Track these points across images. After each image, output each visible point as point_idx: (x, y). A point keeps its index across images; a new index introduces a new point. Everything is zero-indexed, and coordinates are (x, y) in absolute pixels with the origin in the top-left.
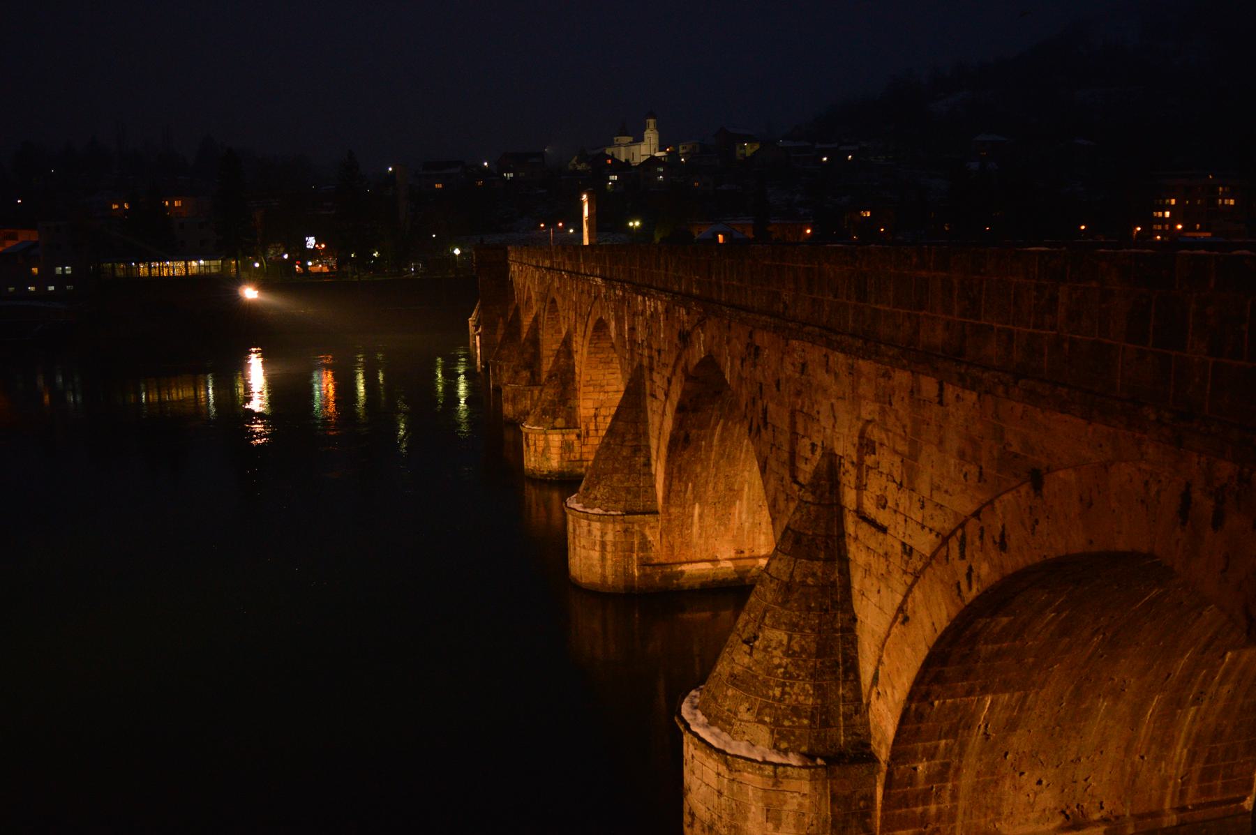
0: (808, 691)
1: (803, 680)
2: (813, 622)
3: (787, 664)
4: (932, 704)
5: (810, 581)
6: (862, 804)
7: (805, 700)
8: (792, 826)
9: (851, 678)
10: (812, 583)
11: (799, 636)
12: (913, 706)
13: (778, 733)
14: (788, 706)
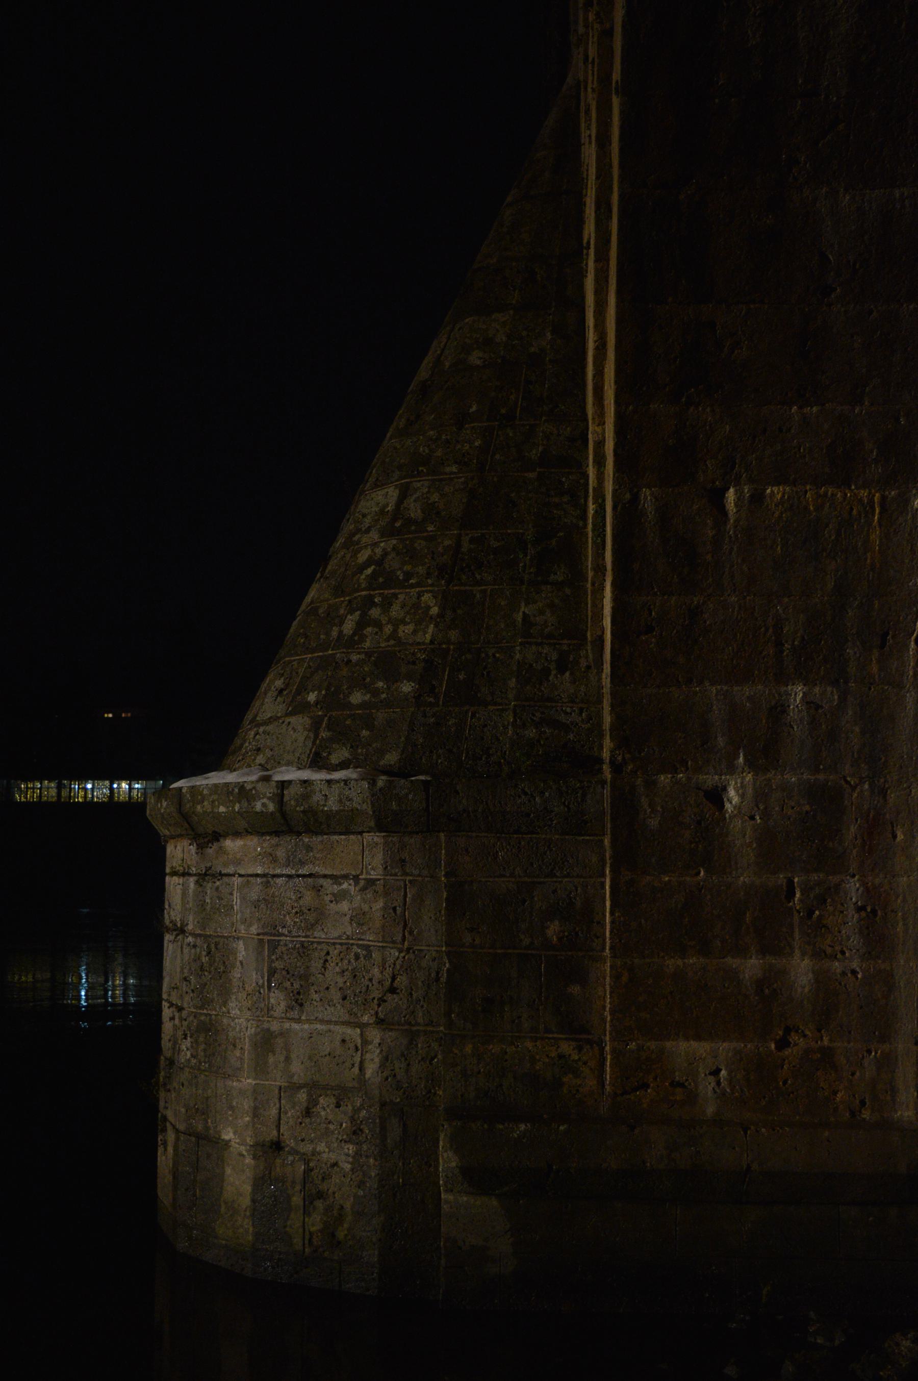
0: (429, 608)
1: (418, 585)
2: (467, 447)
3: (385, 554)
4: (718, 497)
5: (475, 358)
6: (553, 929)
7: (415, 632)
8: (336, 996)
9: (559, 576)
10: (478, 362)
11: (426, 484)
12: (647, 497)
13: (329, 728)
14: (369, 654)
